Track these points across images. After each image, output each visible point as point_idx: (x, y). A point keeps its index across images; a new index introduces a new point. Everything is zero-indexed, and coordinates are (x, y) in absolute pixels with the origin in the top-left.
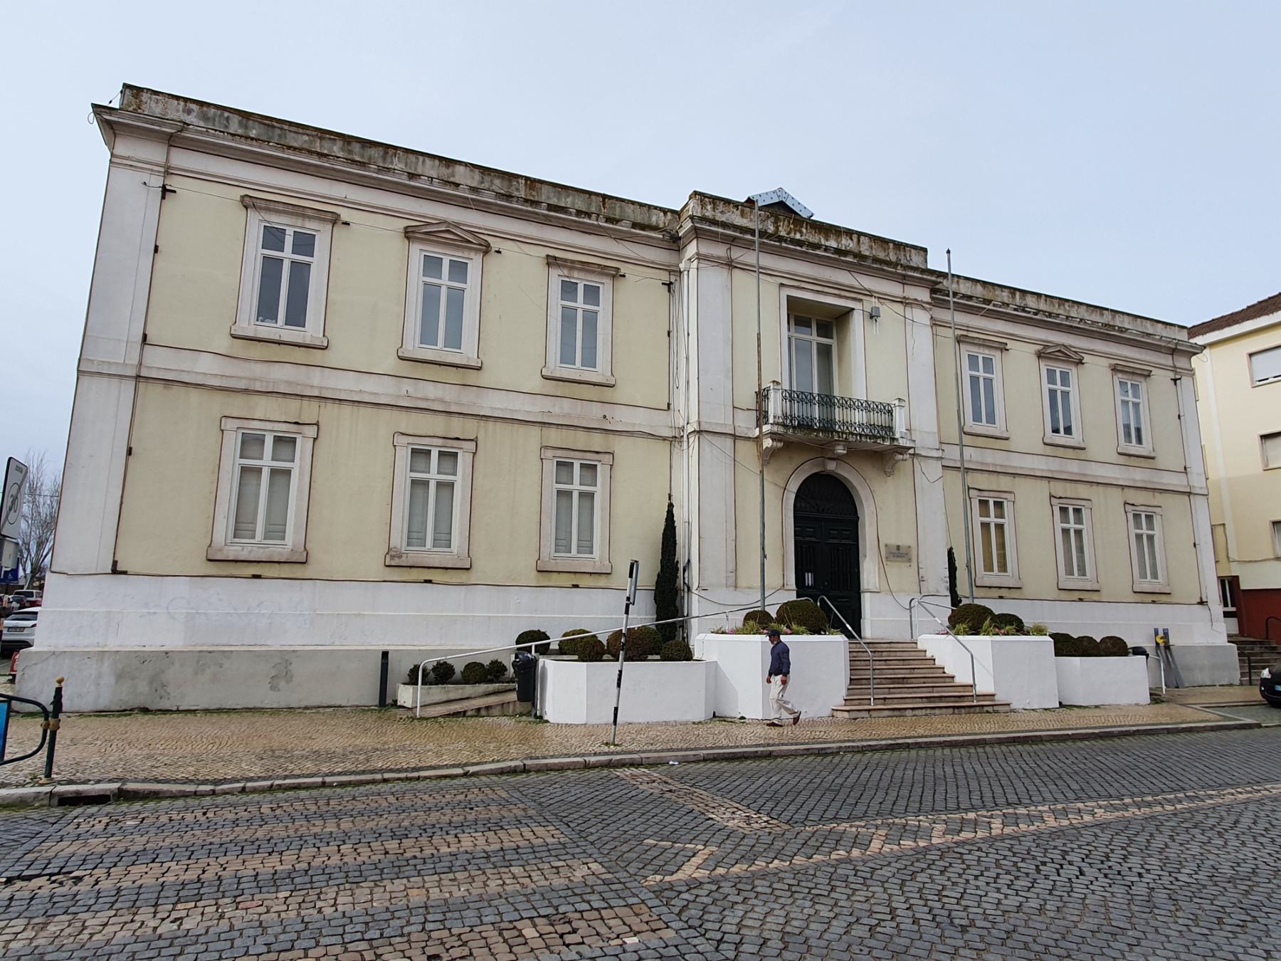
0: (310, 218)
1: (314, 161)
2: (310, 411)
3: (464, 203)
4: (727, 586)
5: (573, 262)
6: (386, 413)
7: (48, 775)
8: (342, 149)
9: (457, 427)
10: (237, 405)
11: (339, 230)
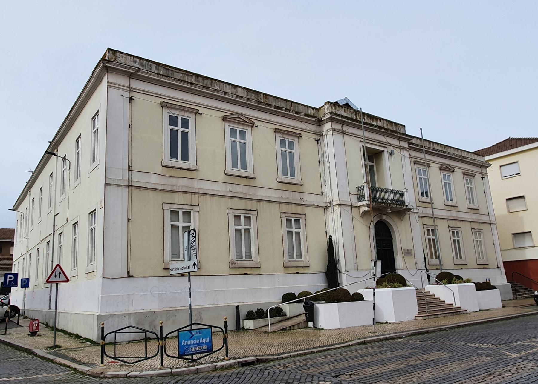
0: (187, 111)
1: (189, 86)
2: (195, 199)
3: (244, 105)
4: (355, 269)
5: (284, 131)
6: (223, 199)
7: (227, 356)
8: (196, 80)
9: (250, 205)
10: (168, 198)
11: (198, 116)
